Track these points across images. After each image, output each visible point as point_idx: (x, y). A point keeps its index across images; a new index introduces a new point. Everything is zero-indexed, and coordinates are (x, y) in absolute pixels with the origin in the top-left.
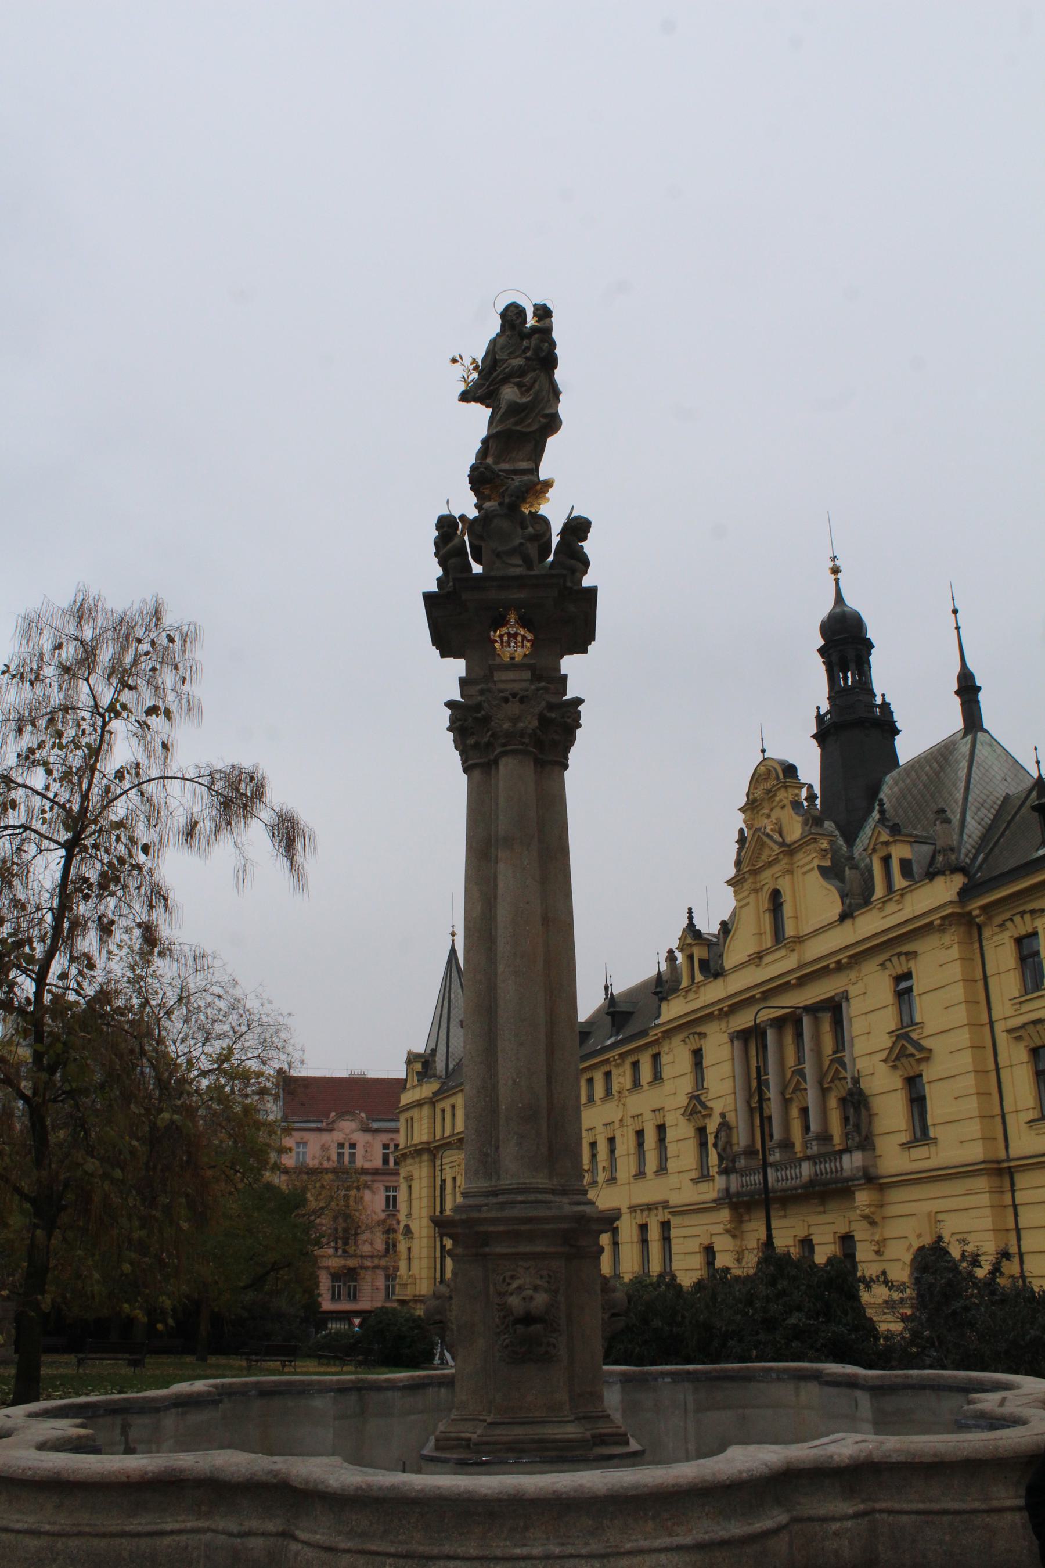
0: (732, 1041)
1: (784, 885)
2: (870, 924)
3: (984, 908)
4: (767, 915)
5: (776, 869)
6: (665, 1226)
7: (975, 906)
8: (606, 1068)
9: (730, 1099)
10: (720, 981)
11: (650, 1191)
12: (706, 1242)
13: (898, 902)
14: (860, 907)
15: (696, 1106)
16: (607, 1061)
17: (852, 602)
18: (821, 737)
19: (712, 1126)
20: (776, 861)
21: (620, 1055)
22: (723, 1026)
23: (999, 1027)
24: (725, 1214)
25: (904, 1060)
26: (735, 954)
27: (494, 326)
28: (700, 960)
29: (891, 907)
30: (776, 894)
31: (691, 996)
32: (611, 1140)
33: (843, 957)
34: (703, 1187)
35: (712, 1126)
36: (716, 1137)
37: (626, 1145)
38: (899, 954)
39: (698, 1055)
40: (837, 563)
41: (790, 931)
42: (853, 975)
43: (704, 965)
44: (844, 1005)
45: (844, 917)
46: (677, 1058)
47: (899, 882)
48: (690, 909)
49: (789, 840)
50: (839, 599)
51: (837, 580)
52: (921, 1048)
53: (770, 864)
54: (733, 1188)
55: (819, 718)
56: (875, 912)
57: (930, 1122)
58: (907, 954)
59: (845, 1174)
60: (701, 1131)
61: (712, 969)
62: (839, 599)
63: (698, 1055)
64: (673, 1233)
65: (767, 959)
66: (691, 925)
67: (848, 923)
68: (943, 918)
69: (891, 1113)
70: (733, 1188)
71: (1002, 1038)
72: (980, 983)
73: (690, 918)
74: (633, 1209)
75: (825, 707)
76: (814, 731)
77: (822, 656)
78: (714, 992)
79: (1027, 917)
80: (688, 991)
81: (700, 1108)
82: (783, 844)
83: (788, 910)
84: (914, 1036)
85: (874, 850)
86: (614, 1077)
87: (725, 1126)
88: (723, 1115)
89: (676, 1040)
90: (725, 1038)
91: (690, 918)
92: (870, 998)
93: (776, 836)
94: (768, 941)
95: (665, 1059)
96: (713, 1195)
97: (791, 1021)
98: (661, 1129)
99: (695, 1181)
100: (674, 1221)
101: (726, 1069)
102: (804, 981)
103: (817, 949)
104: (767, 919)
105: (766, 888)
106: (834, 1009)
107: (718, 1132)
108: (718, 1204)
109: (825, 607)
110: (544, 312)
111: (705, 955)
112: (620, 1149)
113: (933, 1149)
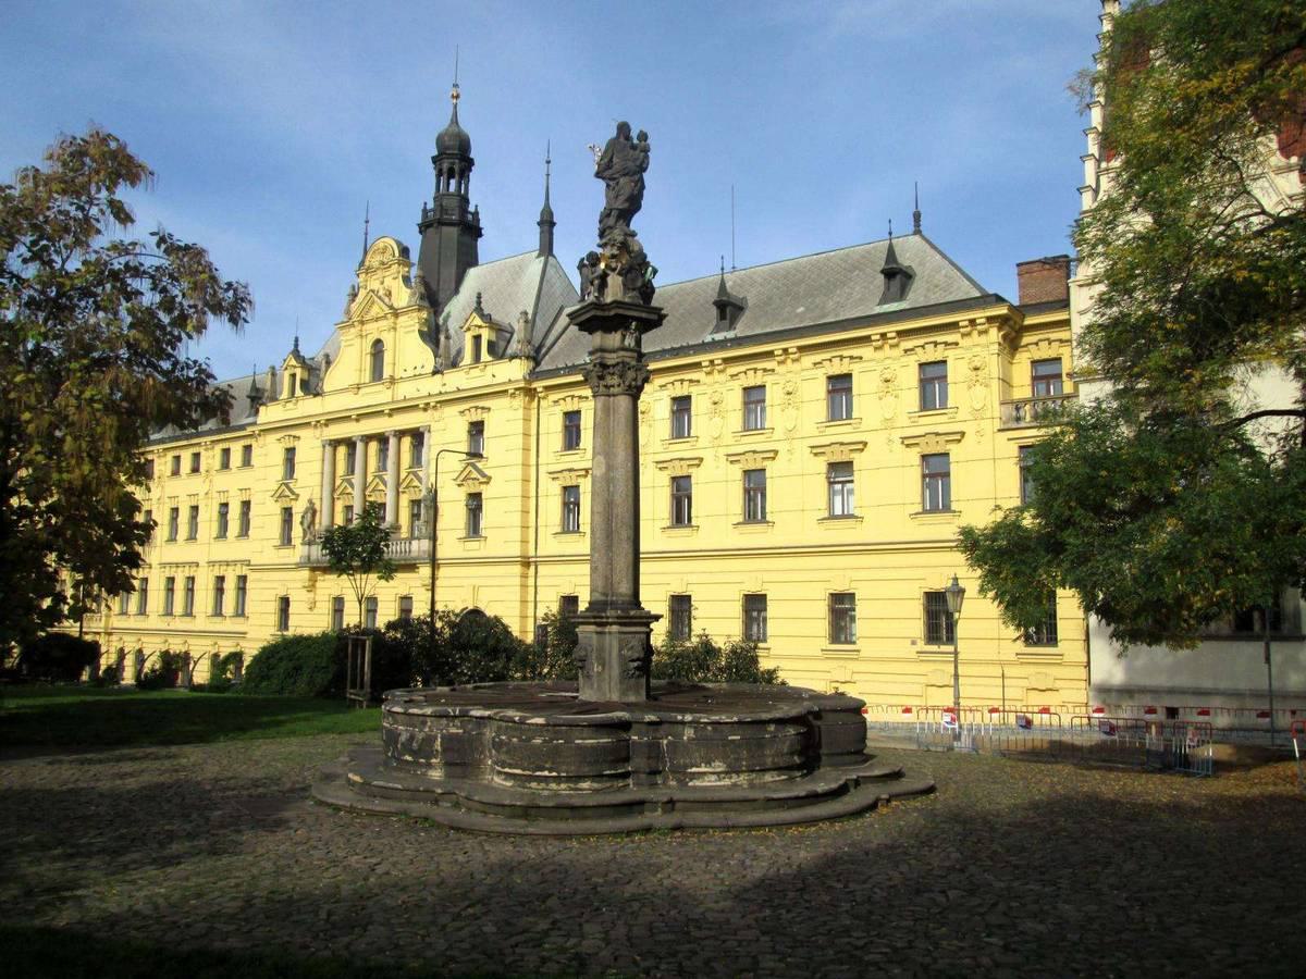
0: (324, 447)
1: (387, 338)
2: (455, 380)
3: (547, 388)
4: (369, 357)
5: (383, 324)
6: (243, 579)
7: (539, 385)
8: (196, 450)
9: (317, 490)
10: (319, 399)
11: (232, 548)
12: (283, 594)
13: (482, 370)
14: (448, 367)
15: (286, 489)
16: (199, 444)
17: (467, 126)
18: (424, 227)
19: (299, 508)
20: (385, 317)
21: (213, 442)
22: (318, 432)
23: (541, 469)
24: (305, 574)
25: (470, 482)
26: (333, 380)
27: (613, 133)
28: (302, 381)
29: (475, 372)
30: (378, 343)
31: (290, 405)
32: (195, 509)
33: (432, 401)
34: (285, 552)
35: (299, 508)
36: (303, 517)
37: (209, 517)
38: (477, 408)
39: (290, 453)
40: (459, 90)
41: (387, 372)
42: (437, 414)
43: (305, 386)
44: (426, 435)
45: (435, 373)
46: (269, 452)
47: (485, 356)
48: (297, 340)
49: (396, 306)
50: (455, 120)
51: (455, 106)
52: (484, 476)
53: (377, 320)
54: (313, 558)
55: (425, 211)
56: (462, 373)
57: (483, 524)
58: (483, 408)
59: (413, 555)
60: (288, 512)
61: (311, 387)
62: (455, 120)
63: (290, 453)
64: (249, 585)
65: (362, 391)
66: (296, 353)
67: (438, 376)
68: (516, 389)
69: (452, 515)
70: (313, 558)
71: (543, 477)
72: (531, 438)
73: (296, 345)
74: (212, 563)
75: (431, 205)
76: (420, 221)
77: (434, 162)
78: (309, 406)
79: (576, 400)
80: (288, 401)
81: (287, 493)
82: (391, 307)
83: (387, 358)
84: (480, 465)
85: (469, 329)
86: (202, 459)
87: (312, 511)
88: (310, 501)
89: (272, 438)
90: (319, 443)
91: (296, 345)
92: (448, 430)
93: (387, 300)
94: (367, 377)
95: (255, 452)
96: (297, 559)
97: (382, 439)
98: (246, 505)
99: (278, 548)
100: (251, 576)
101: (317, 467)
102: (392, 412)
103: (406, 390)
104: (368, 361)
105: (370, 337)
106: (418, 436)
107: (306, 513)
108: (299, 566)
109: (443, 124)
110: (643, 136)
111: (306, 377)
112: (202, 516)
113: (483, 543)
